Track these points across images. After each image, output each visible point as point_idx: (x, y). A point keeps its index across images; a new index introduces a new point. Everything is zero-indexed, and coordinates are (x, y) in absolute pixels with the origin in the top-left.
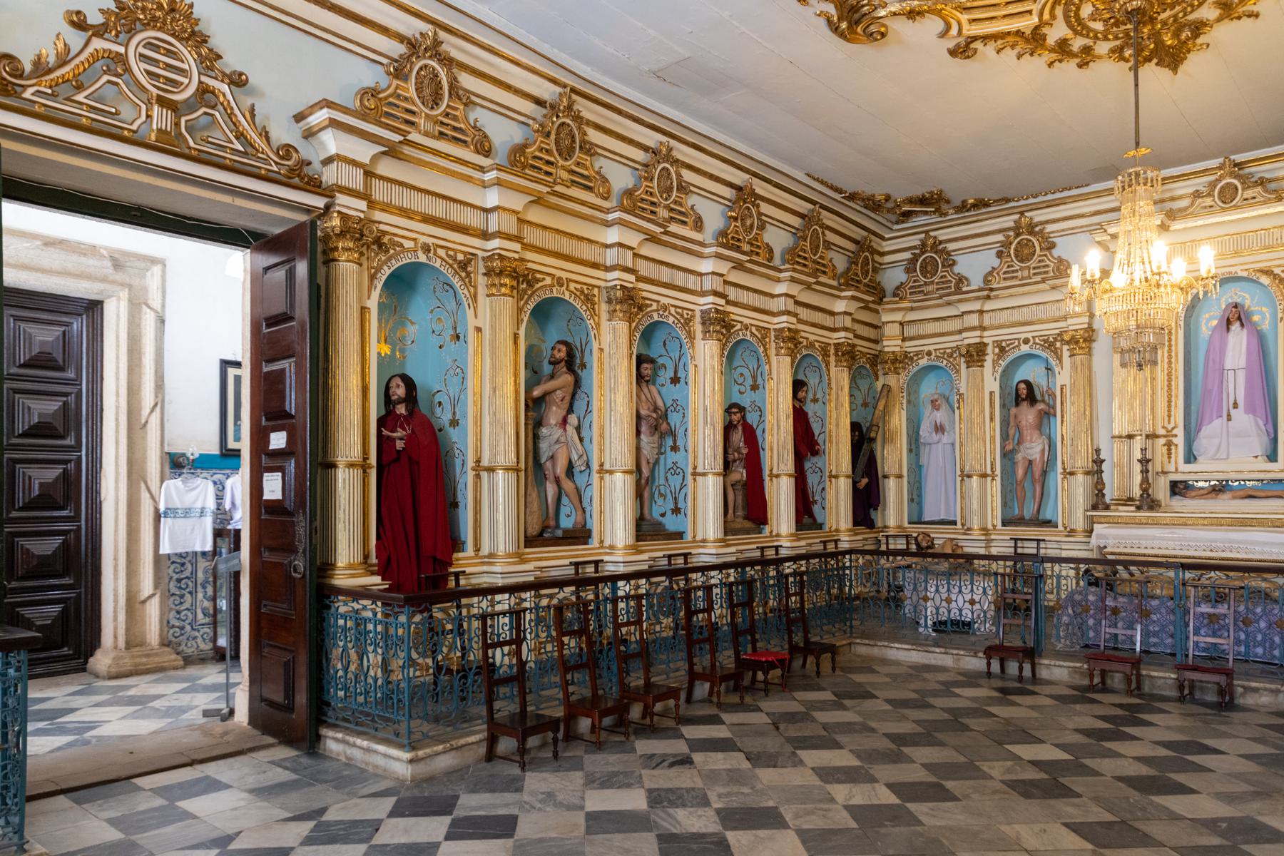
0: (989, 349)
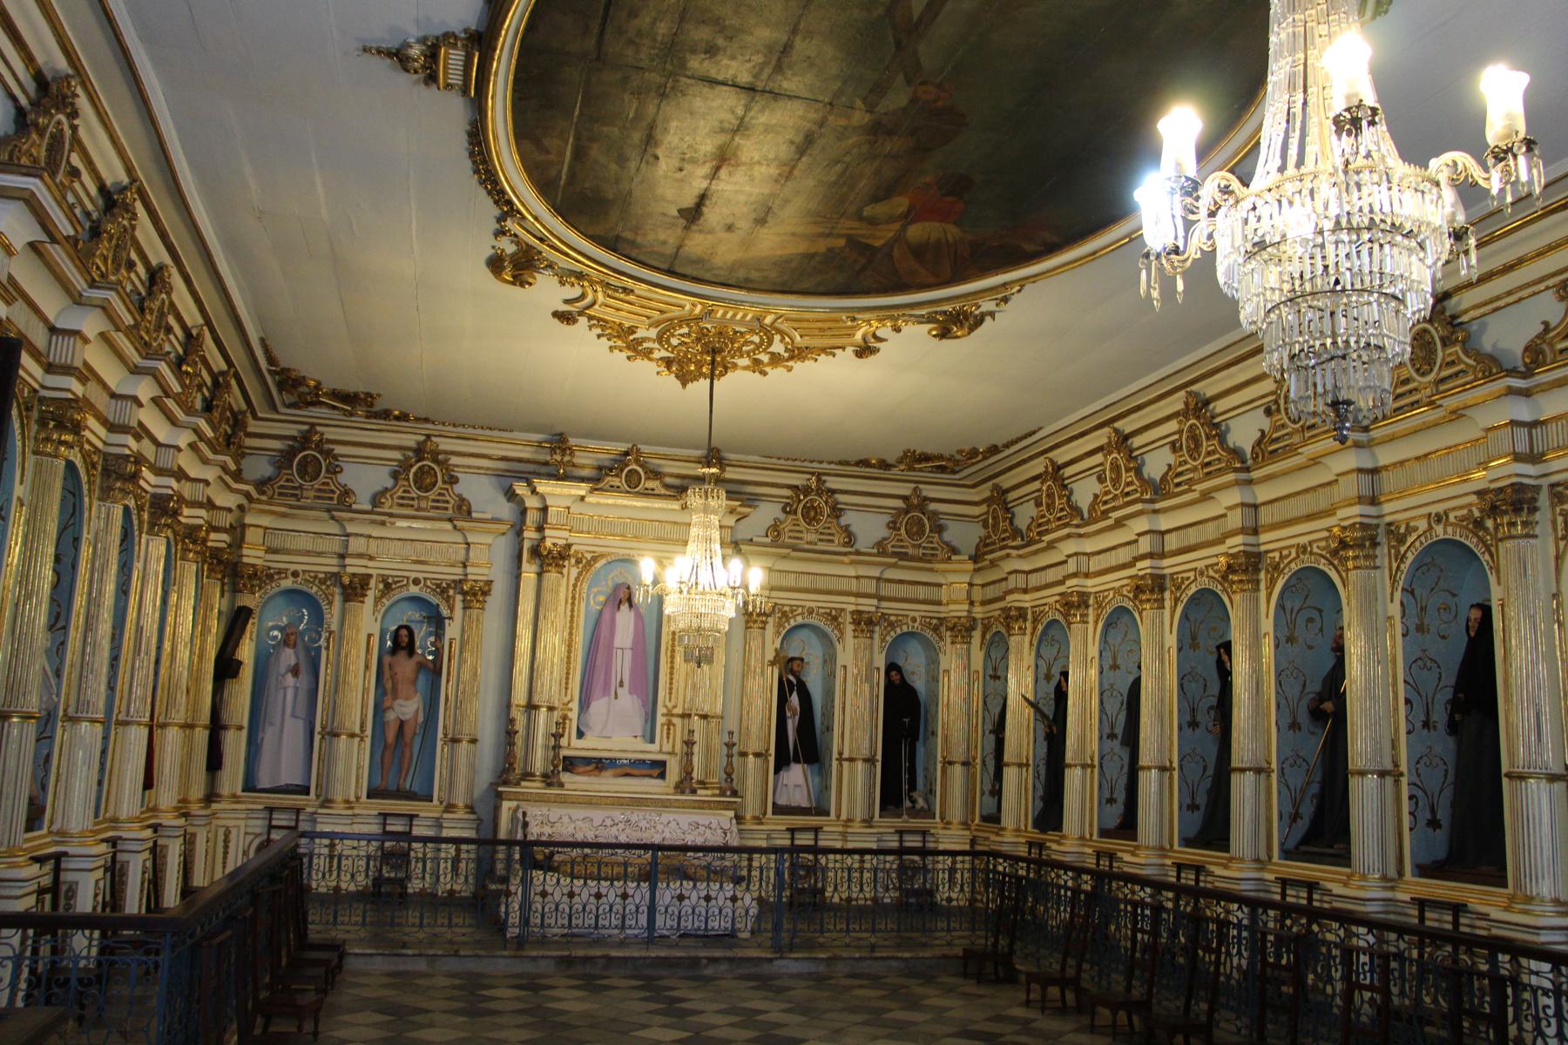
0: (372, 583)
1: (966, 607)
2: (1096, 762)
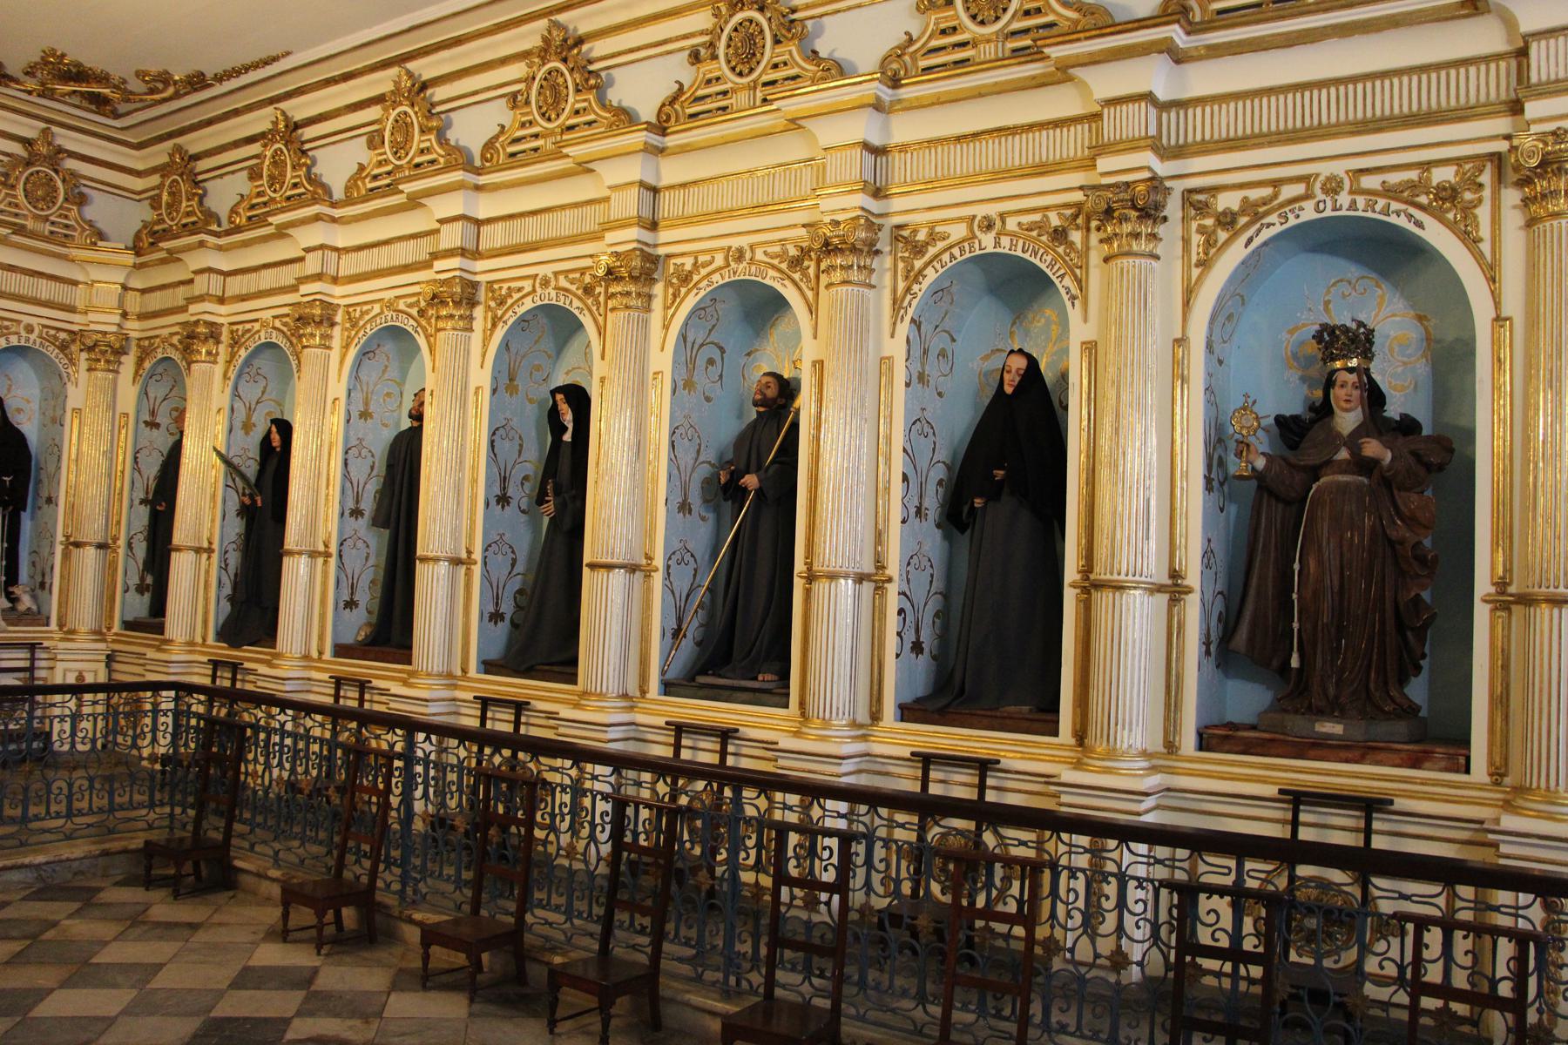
1: (117, 319)
2: (333, 549)
